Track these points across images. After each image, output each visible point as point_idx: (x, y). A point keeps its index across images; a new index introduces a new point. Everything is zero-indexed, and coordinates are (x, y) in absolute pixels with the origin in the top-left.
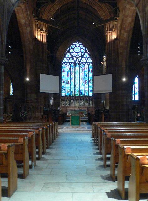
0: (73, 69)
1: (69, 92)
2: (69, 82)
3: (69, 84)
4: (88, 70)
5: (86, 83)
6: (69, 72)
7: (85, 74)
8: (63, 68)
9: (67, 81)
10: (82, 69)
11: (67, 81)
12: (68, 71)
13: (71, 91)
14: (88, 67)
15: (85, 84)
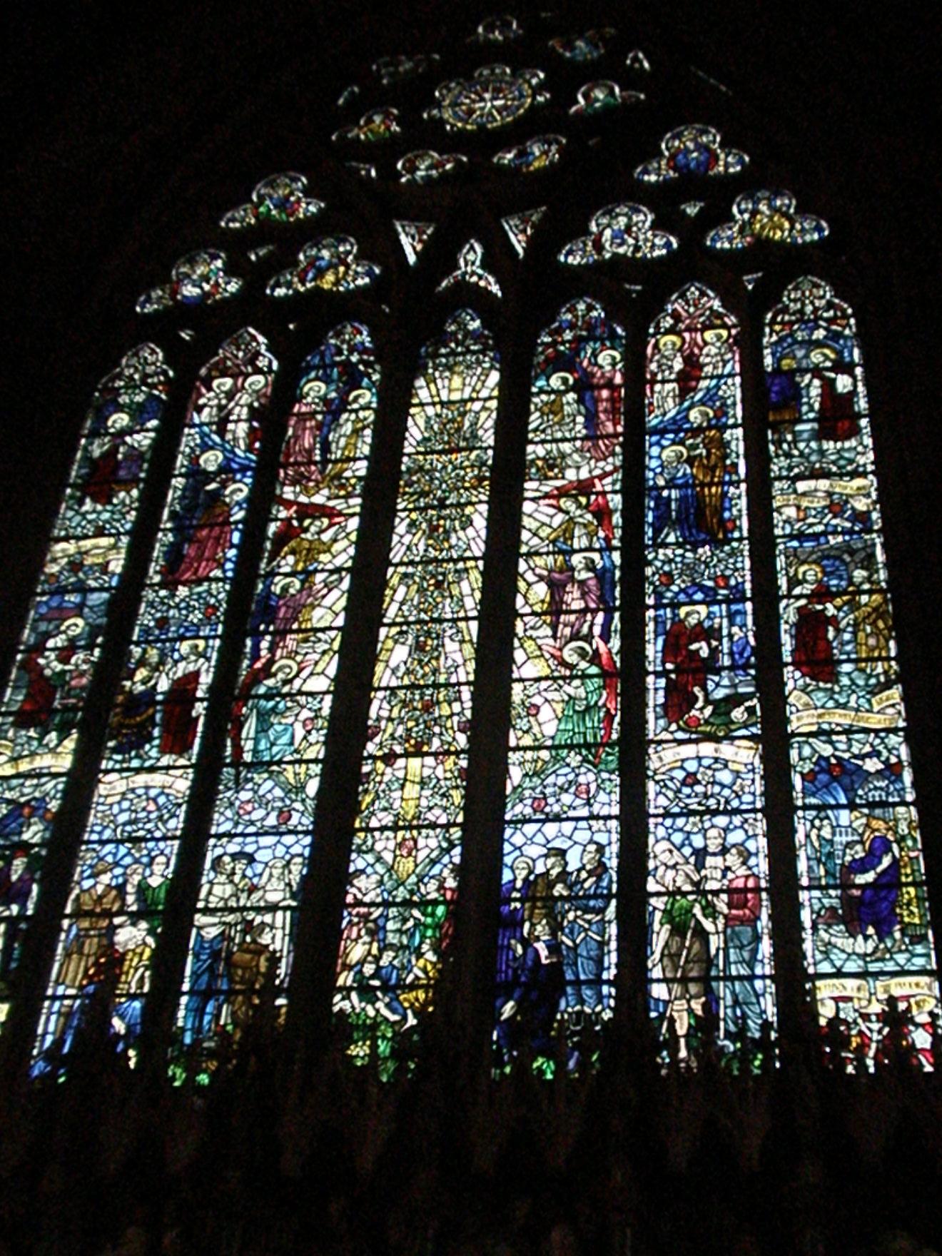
0: (335, 409)
1: (136, 977)
2: (184, 689)
3: (177, 742)
4: (734, 390)
5: (678, 703)
6: (239, 491)
7: (654, 476)
8: (120, 420)
9: (137, 683)
10: (585, 387)
11: (137, 683)
12: (211, 461)
13: (208, 927)
14: (748, 345)
15: (654, 725)
